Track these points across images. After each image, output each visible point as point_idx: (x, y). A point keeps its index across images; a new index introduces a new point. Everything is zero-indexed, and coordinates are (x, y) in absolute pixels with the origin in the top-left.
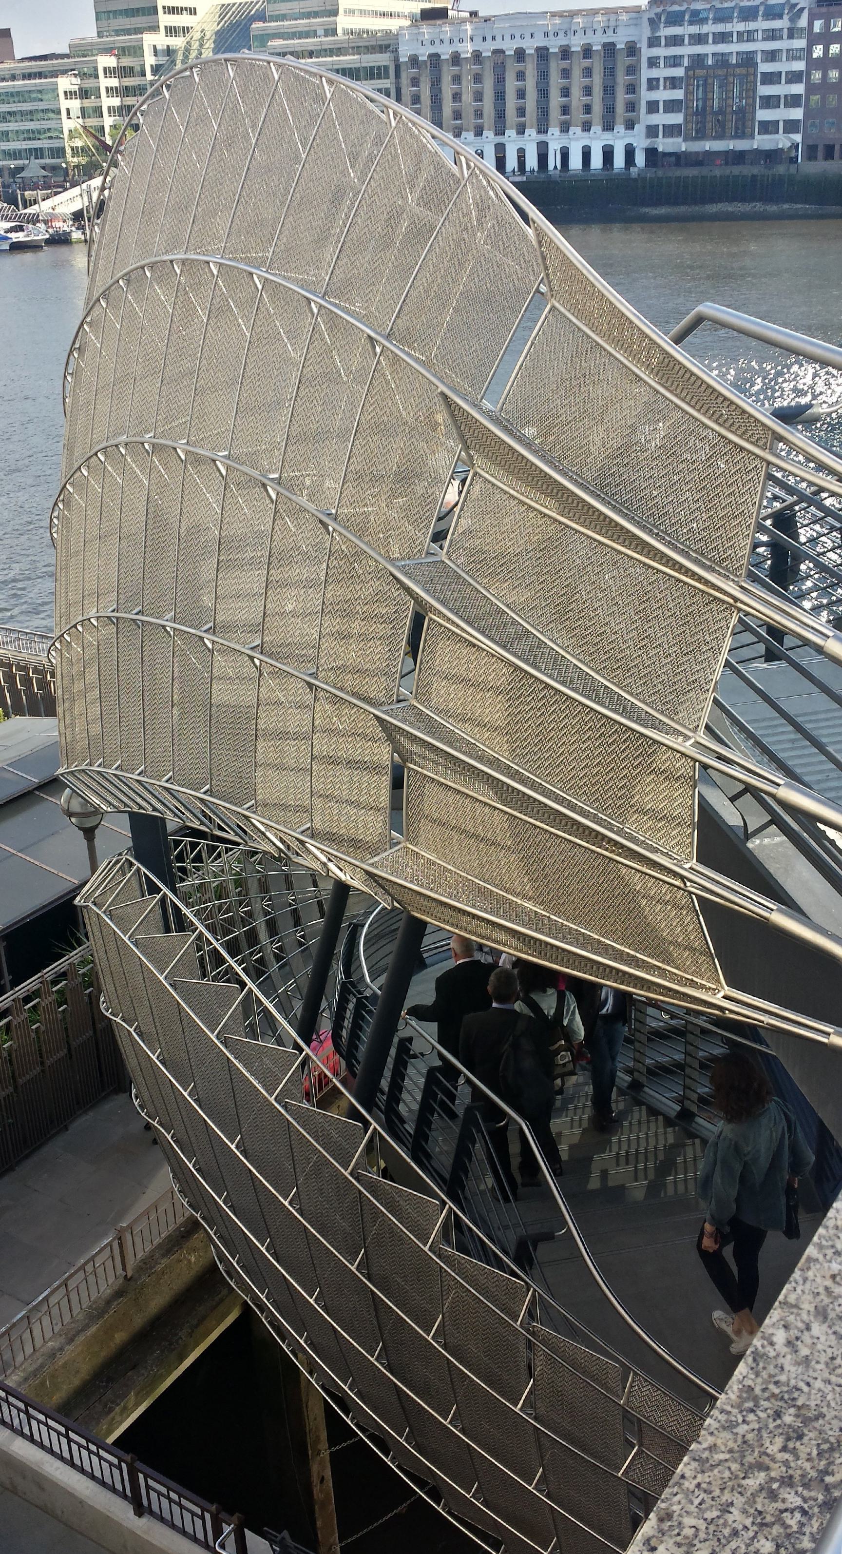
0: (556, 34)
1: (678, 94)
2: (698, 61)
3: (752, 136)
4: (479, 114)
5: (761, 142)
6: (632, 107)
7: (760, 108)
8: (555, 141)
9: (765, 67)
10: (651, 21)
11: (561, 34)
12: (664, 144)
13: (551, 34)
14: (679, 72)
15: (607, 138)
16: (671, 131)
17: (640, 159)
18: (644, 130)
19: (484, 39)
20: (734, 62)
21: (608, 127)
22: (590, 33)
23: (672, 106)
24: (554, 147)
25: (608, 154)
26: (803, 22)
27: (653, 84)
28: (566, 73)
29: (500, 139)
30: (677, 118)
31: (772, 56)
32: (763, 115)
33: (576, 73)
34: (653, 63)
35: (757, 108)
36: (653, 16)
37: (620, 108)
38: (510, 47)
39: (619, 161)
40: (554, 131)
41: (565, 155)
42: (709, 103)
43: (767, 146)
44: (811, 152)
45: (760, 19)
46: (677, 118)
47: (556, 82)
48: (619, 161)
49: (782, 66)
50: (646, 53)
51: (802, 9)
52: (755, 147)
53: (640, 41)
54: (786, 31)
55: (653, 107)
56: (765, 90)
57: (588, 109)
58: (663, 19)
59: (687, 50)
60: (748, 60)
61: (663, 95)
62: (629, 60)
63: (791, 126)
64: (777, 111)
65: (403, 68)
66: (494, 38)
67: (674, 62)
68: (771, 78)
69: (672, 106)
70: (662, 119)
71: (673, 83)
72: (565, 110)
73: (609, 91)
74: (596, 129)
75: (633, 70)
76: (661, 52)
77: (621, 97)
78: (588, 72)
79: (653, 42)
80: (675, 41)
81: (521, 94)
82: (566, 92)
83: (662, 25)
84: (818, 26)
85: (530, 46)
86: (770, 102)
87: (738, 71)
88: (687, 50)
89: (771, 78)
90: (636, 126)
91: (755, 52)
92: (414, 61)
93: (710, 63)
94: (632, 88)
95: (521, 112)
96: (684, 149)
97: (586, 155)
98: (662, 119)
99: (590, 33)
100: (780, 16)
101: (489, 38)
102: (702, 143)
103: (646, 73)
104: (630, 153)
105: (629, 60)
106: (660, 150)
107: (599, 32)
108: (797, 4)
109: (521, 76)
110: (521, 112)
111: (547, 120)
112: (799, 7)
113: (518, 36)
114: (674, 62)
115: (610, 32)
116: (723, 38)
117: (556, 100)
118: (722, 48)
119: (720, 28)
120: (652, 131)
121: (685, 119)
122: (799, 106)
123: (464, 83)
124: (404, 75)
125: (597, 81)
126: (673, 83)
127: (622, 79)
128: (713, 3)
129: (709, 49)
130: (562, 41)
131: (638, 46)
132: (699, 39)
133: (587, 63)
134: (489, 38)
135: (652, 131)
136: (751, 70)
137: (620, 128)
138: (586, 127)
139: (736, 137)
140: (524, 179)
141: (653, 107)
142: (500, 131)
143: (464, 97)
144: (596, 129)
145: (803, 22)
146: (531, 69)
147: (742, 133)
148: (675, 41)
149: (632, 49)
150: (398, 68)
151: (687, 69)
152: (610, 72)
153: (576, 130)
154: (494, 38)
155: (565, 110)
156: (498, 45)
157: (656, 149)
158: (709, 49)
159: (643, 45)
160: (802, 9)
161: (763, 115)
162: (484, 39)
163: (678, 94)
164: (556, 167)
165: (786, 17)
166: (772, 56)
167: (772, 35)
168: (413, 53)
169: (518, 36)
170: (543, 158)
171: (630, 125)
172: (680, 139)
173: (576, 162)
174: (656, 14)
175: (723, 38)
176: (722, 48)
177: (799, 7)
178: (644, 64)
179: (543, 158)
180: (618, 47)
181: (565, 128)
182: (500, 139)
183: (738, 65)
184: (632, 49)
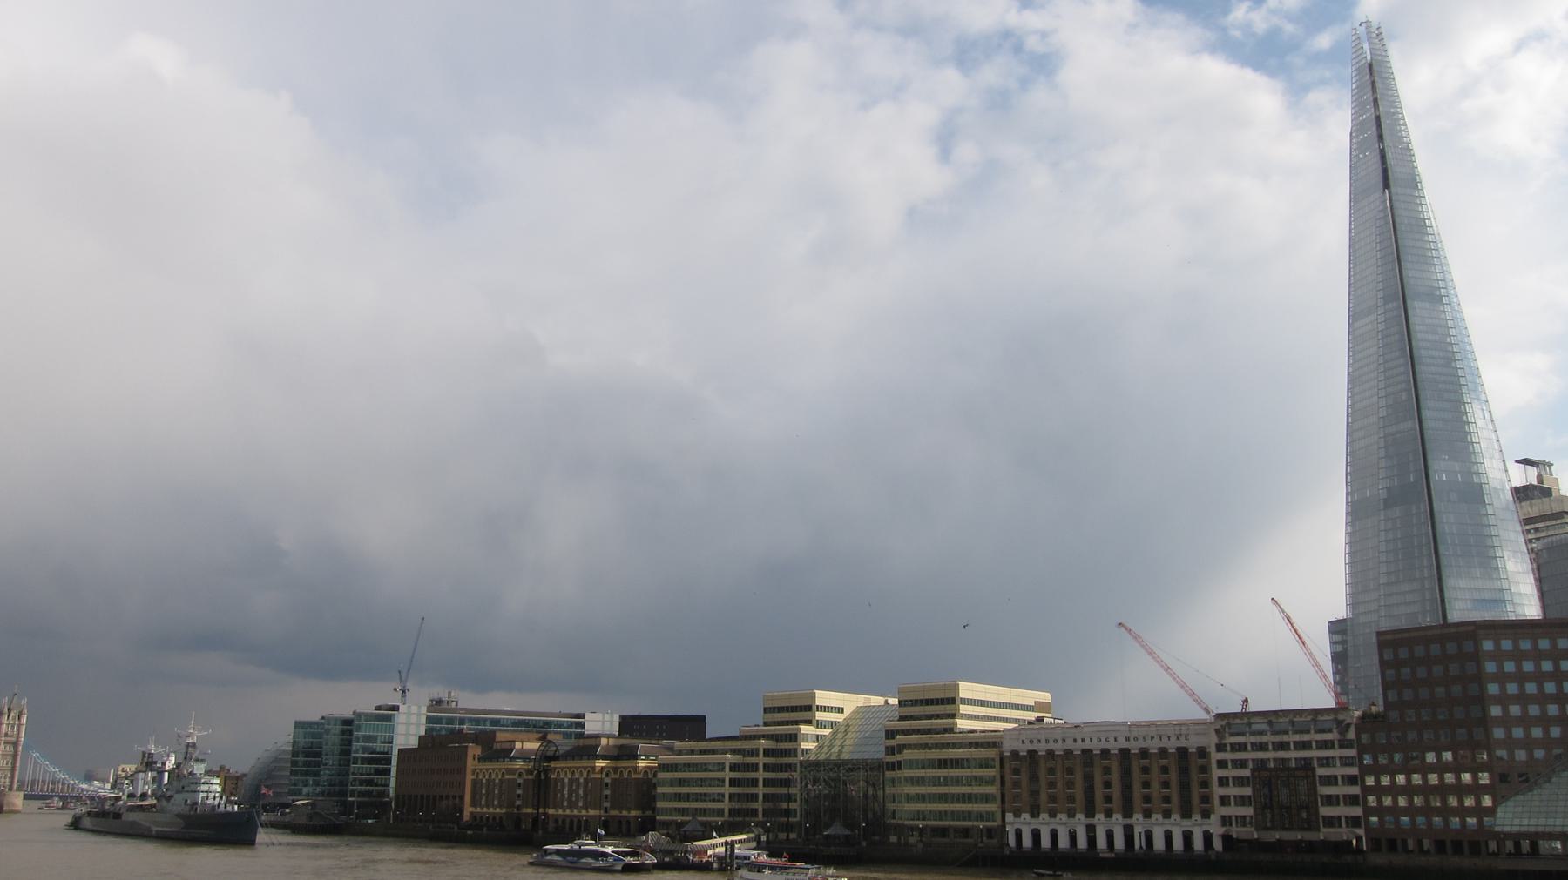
1: (1247, 791)
2: (1261, 765)
3: (1318, 830)
4: (1071, 799)
5: (1325, 833)
6: (1206, 799)
7: (1322, 805)
8: (1139, 824)
9: (1321, 771)
10: (1217, 731)
11: (1141, 740)
12: (1236, 831)
13: (1132, 739)
14: (1246, 773)
15: (1187, 824)
16: (1242, 820)
17: (1218, 845)
18: (1219, 819)
19: (1075, 741)
20: (1294, 765)
21: (1186, 814)
22: (1165, 739)
23: (1242, 801)
24: (1138, 830)
25: (1188, 837)
26: (1351, 735)
27: (1223, 782)
28: (1145, 770)
29: (1090, 821)
30: (1248, 811)
31: (1326, 762)
32: (1325, 811)
33: (1155, 770)
34: (1222, 764)
35: (1320, 804)
36: (1218, 727)
37: (1196, 800)
38: (1096, 747)
39: (1198, 845)
40: (1138, 817)
41: (1149, 836)
43: (1333, 839)
44: (1376, 844)
45: (1312, 732)
46: (1248, 811)
47: (1137, 778)
48: (1198, 845)
49: (1340, 771)
50: (1216, 756)
51: (1349, 725)
52: (1322, 838)
53: (1209, 747)
54: (1336, 743)
55: (1224, 800)
57: (1167, 799)
58: (1227, 729)
59: (1249, 755)
60: (1306, 765)
61: (1233, 791)
62: (1201, 762)
63: (1354, 822)
64: (1339, 808)
65: (1006, 760)
66: (1083, 740)
67: (1241, 764)
68: (1330, 780)
69: (1242, 801)
70: (1233, 810)
71: (1240, 781)
72: (1147, 799)
73: (1185, 786)
74: (1176, 817)
75: (1205, 769)
76: (1228, 756)
77: (1196, 793)
78: (1165, 770)
79: (1220, 748)
80: (1242, 747)
81: (1107, 785)
82: (1146, 785)
83: (1227, 735)
85: (1113, 747)
86: (1331, 800)
88: (1249, 755)
89: (1330, 780)
90: (1212, 816)
91: (1311, 759)
92: (1015, 754)
93: (1272, 765)
94: (1205, 784)
95: (1108, 799)
96: (1256, 837)
97: (1168, 837)
98: (1233, 810)
99: (1165, 739)
100: (1330, 731)
101: (1079, 740)
102: (1273, 832)
103: (1217, 773)
104: (1208, 837)
105: (1201, 762)
106: (1235, 836)
107: (1173, 739)
108: (1344, 720)
109: (1107, 770)
110: (1108, 799)
112: (1346, 722)
113: (1103, 739)
114: (1241, 764)
115: (1183, 738)
116: (1283, 746)
117: (1138, 792)
119: (1277, 738)
120: (1225, 820)
121: (1255, 811)
123: (1059, 774)
124: (1007, 766)
125: (1173, 776)
126: (1240, 781)
127: (1195, 777)
131: (1208, 750)
132: (1262, 747)
133: (1164, 762)
134: (1079, 740)
135: (1225, 820)
136: (1310, 773)
137: (1197, 817)
138: (1167, 815)
139: (1303, 829)
140: (1113, 855)
141: (1224, 800)
142: (1090, 813)
143: (1059, 785)
144: (1176, 817)
145: (1351, 735)
146: (1115, 766)
147: (1311, 825)
148: (1242, 747)
150: (1002, 760)
151: (1253, 771)
152: (1184, 771)
153: (1158, 817)
154: (1083, 740)
155: (1147, 799)
156: (1087, 745)
157: (1231, 836)
159: (1212, 750)
160: (1349, 725)
161: (1325, 811)
162: (1075, 741)
163: (1247, 791)
164: (1141, 847)
165: (1335, 731)
166: (1326, 762)
168: (1015, 749)
169: (1103, 739)
170: (1129, 838)
171: (1206, 814)
172: (1253, 829)
173: (1159, 844)
174: (1222, 726)
175: (1283, 746)
178: (1214, 765)
179: (1129, 838)
180: (1190, 751)
181: (1147, 814)
182: (1090, 821)
183: (1297, 769)
184: (1203, 752)
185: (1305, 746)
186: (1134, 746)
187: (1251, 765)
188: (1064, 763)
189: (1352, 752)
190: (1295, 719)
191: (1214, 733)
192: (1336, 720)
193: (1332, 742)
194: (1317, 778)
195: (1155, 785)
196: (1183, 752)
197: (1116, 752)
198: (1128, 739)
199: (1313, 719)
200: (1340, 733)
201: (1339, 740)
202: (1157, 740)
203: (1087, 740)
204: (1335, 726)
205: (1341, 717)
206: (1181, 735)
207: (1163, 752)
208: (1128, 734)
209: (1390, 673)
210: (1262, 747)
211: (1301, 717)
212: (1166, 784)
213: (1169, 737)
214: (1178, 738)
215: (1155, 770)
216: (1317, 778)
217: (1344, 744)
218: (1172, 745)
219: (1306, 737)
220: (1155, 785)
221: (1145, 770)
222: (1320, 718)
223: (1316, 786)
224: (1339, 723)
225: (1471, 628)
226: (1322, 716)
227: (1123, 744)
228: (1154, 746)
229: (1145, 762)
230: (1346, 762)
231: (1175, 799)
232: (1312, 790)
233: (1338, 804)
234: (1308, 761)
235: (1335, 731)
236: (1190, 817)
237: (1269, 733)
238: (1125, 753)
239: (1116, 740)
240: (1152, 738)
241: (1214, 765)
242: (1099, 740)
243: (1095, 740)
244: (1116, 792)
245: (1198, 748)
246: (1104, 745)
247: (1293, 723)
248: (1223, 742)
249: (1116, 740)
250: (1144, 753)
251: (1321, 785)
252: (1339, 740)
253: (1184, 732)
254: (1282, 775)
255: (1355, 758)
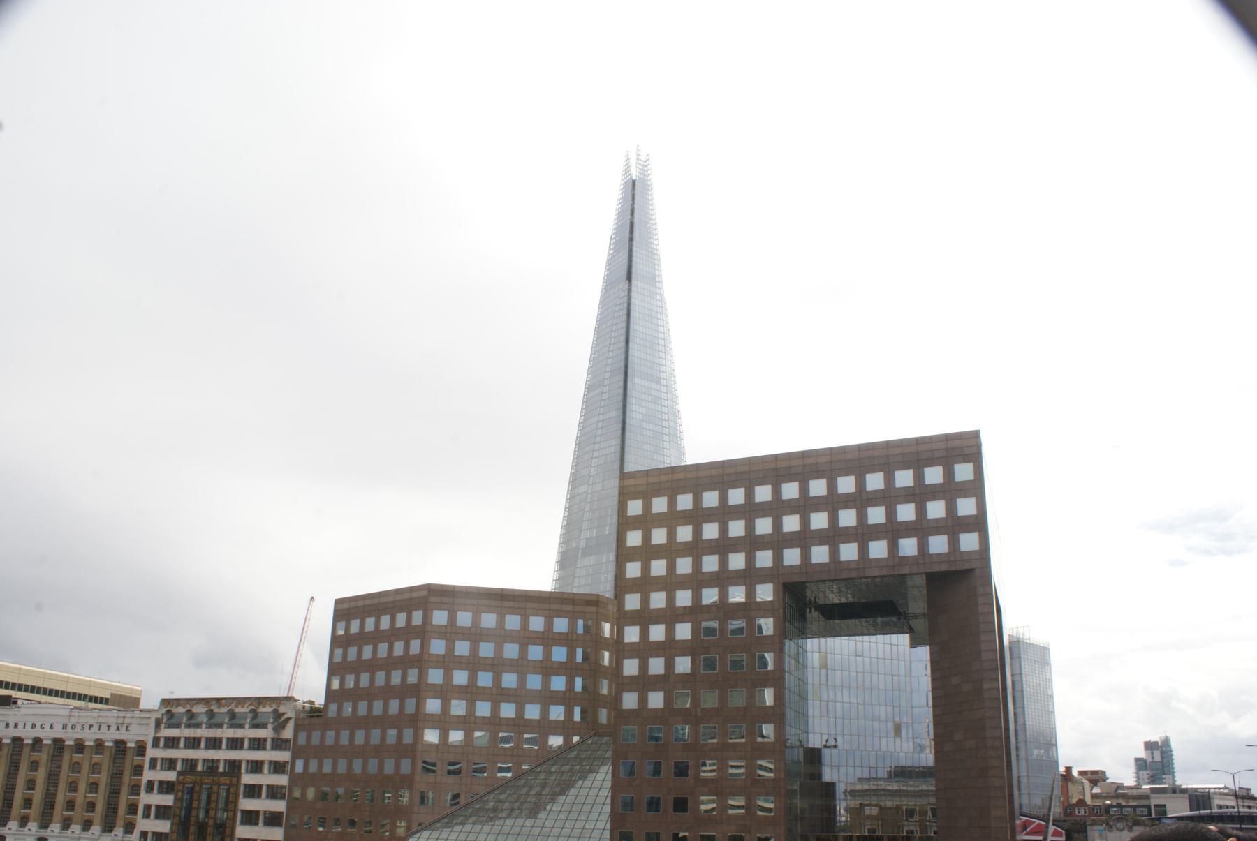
0: (74, 727)
2: (191, 764)
6: (133, 809)
9: (248, 779)
11: (79, 727)
13: (69, 727)
14: (171, 776)
19: (7, 725)
22: (104, 728)
26: (288, 733)
31: (256, 767)
33: (86, 768)
35: (238, 823)
38: (28, 735)
42: (194, 813)
45: (247, 726)
49: (266, 779)
50: (151, 753)
51: (288, 719)
54: (269, 742)
56: (247, 804)
57: (91, 806)
59: (181, 754)
61: (157, 799)
64: (255, 828)
66: (16, 726)
68: (253, 791)
69: (162, 812)
75: (138, 770)
78: (95, 767)
80: (172, 743)
81: (31, 784)
82: (73, 787)
84: (302, 740)
85: (47, 736)
87: (223, 780)
88: (181, 754)
89: (253, 791)
95: (28, 803)
99: (104, 728)
100: (264, 726)
101: (12, 725)
103: (148, 775)
105: (138, 760)
107: (113, 728)
108: (283, 714)
110: (28, 803)
111: (51, 815)
112: (285, 716)
114: (170, 764)
115: (123, 729)
116: (214, 743)
118: (212, 754)
121: (172, 828)
122: (279, 825)
125: (103, 778)
127: (127, 778)
128: (212, 708)
129: (201, 754)
130: (78, 734)
132: (193, 743)
134: (12, 725)
136: (234, 780)
138: (87, 825)
145: (288, 733)
148: (172, 743)
149: (141, 749)
151: (180, 774)
154: (16, 726)
155: (70, 805)
156: (18, 733)
158: (201, 754)
160: (288, 719)
162: (7, 725)
163: (168, 800)
165: (270, 726)
166: (256, 767)
167: (258, 744)
175: (214, 743)
176: (212, 754)
177: (285, 716)
180: (129, 745)
183: (224, 774)
184: (141, 749)
185: (235, 744)
186: (70, 737)
187: (179, 767)
188: (71, 757)
189: (284, 756)
190: (237, 710)
191: (153, 725)
192: (276, 711)
193: (265, 740)
194: (242, 788)
195: (82, 787)
196: (120, 745)
197: (49, 742)
198: (65, 727)
199: (252, 711)
200: (276, 730)
201: (273, 739)
202: (95, 729)
203: (21, 726)
204: (271, 720)
205: (282, 709)
206: (122, 724)
207: (99, 745)
208: (65, 722)
209: (339, 652)
210: (193, 743)
211: (242, 707)
212: (94, 787)
213: (109, 726)
214: (118, 729)
215: (86, 768)
216: (242, 788)
217: (279, 744)
218: (109, 737)
219: (239, 733)
220: (82, 787)
221: (76, 767)
222: (262, 709)
223: (239, 796)
224: (277, 715)
225: (424, 593)
226: (264, 707)
227: (58, 733)
228: (89, 737)
229: (77, 757)
230: (278, 767)
231: (100, 807)
232: (231, 803)
233: (257, 824)
234: (234, 766)
235: (270, 726)
236: (110, 831)
237: (204, 726)
238: (58, 742)
239: (51, 727)
240: (91, 726)
241: (147, 766)
242: (34, 726)
243: (29, 726)
244: (38, 796)
245: (138, 742)
246: (38, 733)
247: (233, 715)
248: (158, 735)
249: (51, 727)
250: (80, 746)
251: (245, 797)
252: (273, 739)
253: (127, 721)
254: (206, 781)
255: (288, 762)
